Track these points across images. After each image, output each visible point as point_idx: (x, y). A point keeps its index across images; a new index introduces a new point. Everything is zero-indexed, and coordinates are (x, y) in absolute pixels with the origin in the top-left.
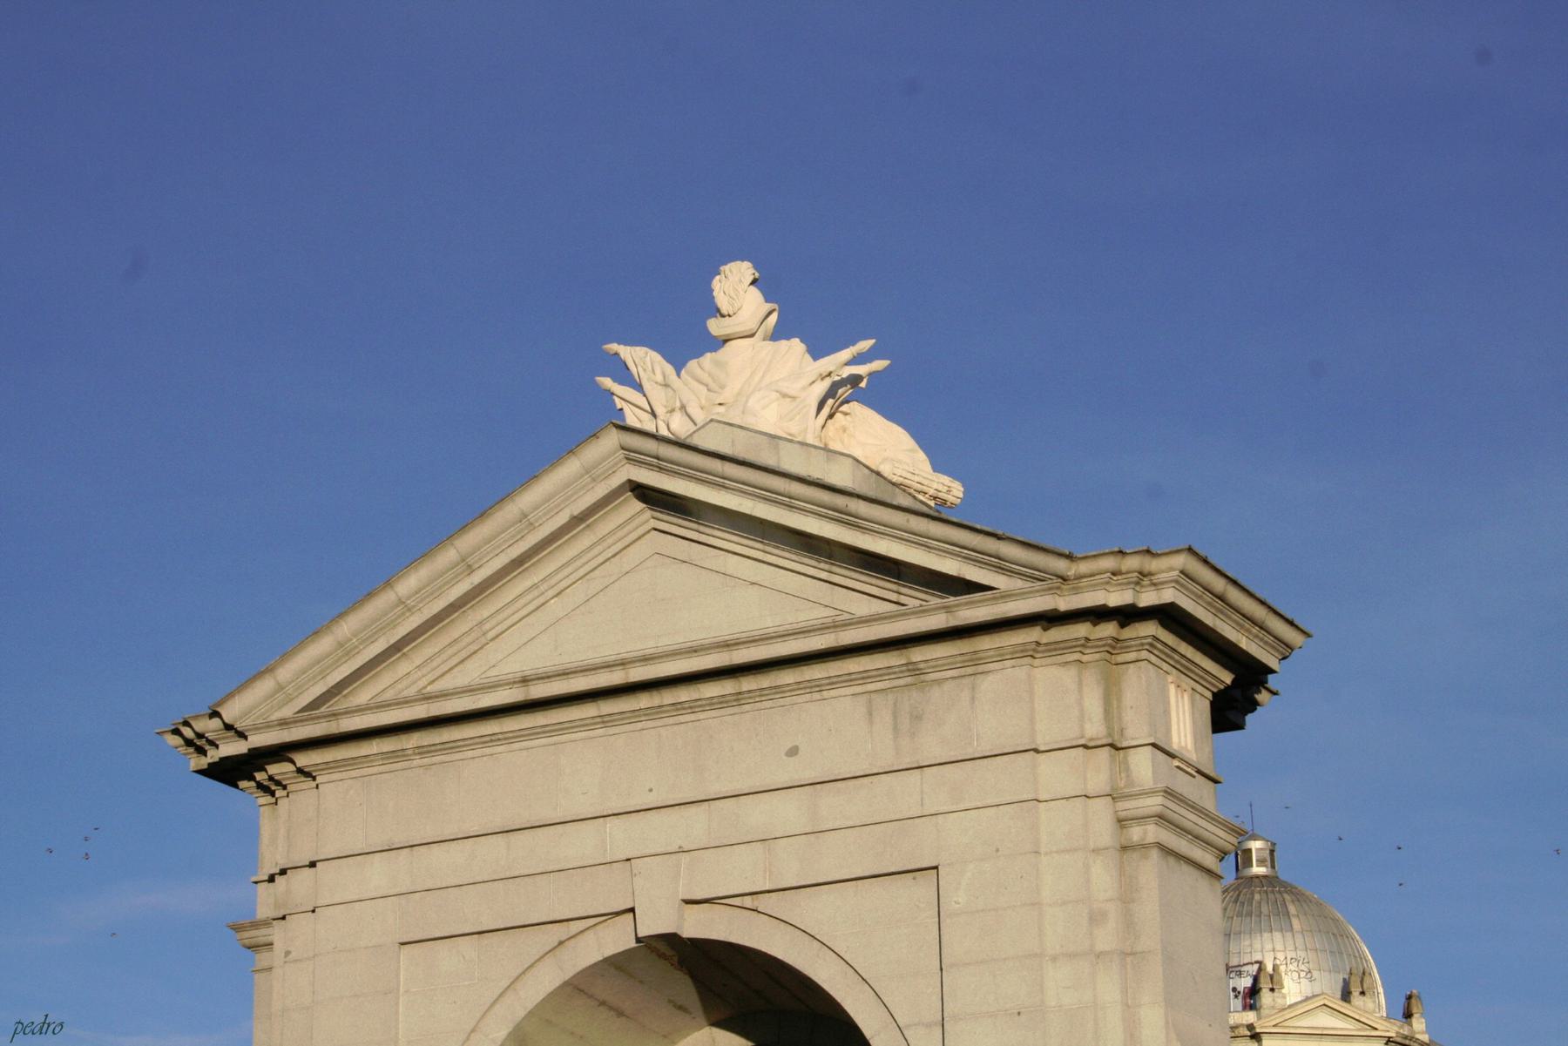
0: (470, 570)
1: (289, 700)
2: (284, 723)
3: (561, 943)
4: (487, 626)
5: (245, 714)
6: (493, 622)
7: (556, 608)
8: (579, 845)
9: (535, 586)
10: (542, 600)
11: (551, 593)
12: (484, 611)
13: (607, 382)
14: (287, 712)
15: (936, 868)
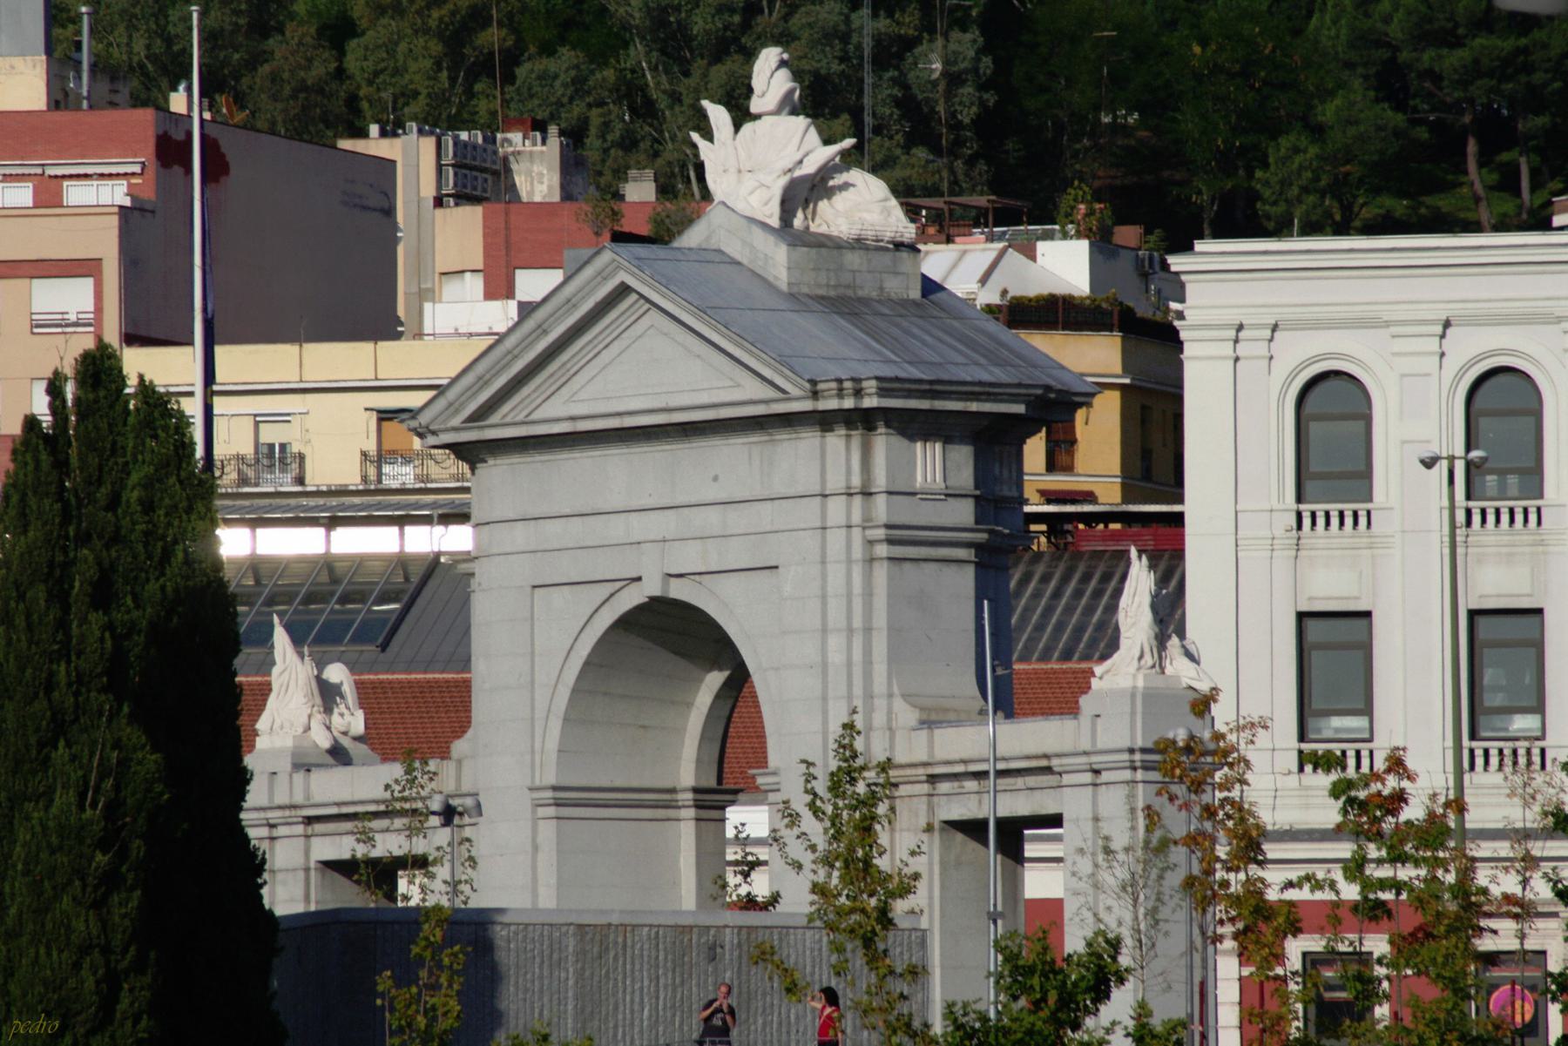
0: (545, 332)
1: (457, 411)
2: (455, 429)
3: (612, 595)
4: (569, 366)
5: (433, 421)
6: (572, 363)
7: (606, 356)
8: (617, 528)
9: (590, 341)
10: (596, 351)
11: (601, 346)
12: (564, 357)
13: (695, 136)
14: (456, 421)
15: (776, 567)
